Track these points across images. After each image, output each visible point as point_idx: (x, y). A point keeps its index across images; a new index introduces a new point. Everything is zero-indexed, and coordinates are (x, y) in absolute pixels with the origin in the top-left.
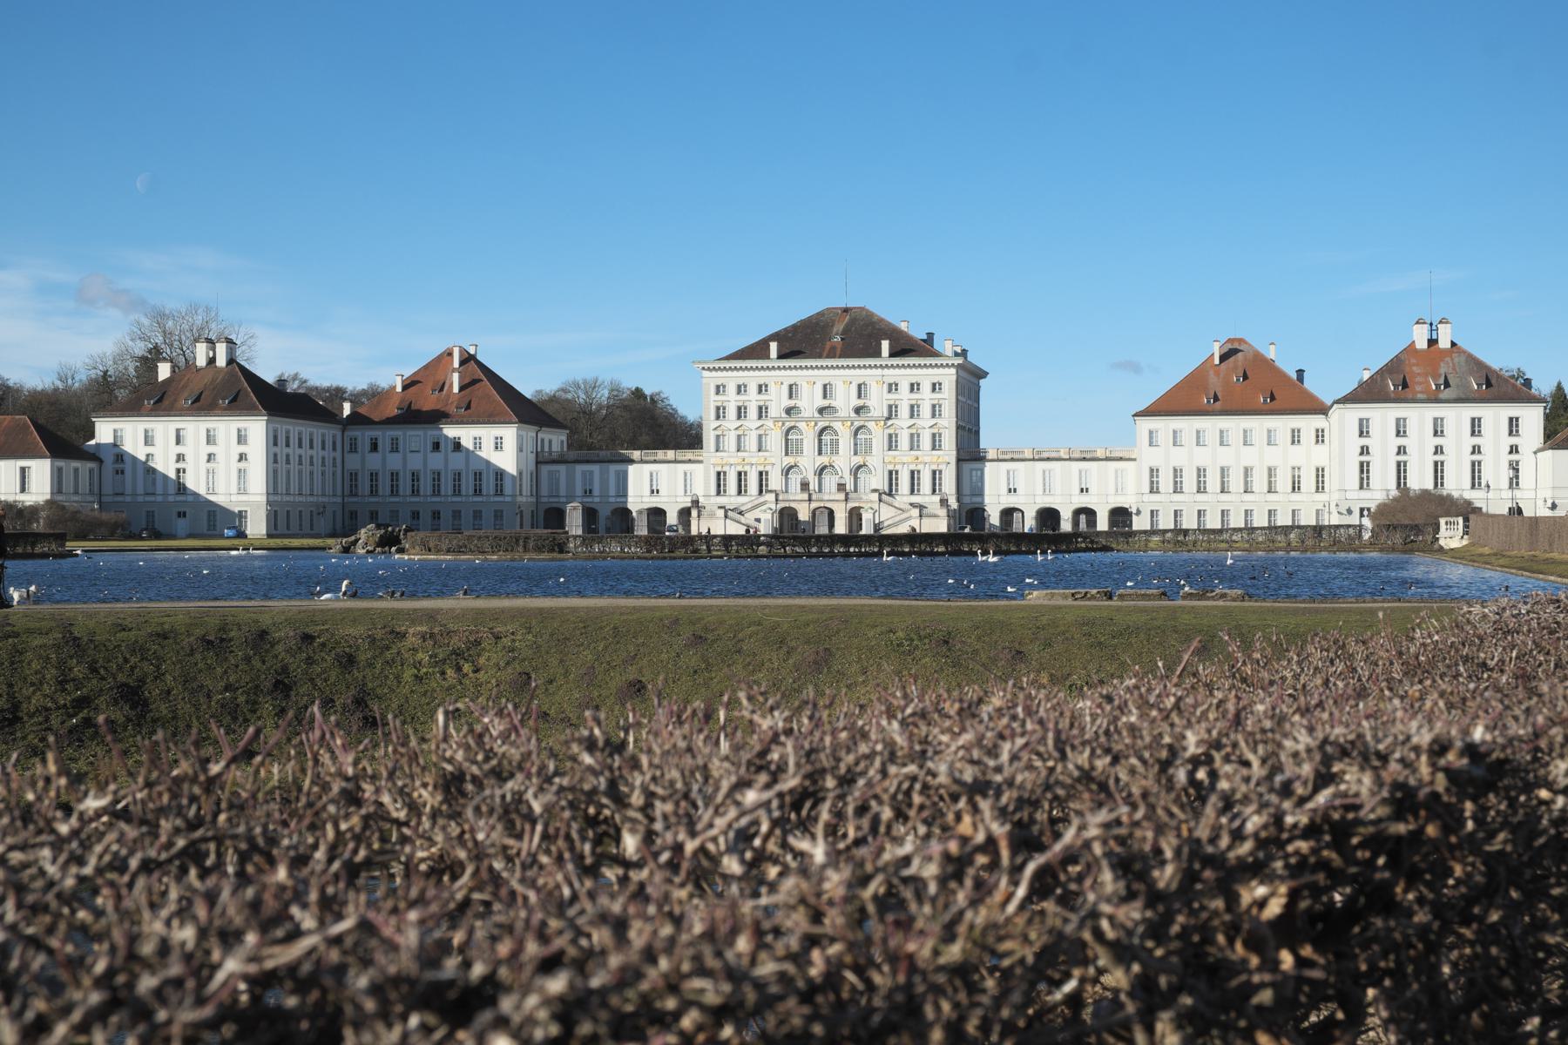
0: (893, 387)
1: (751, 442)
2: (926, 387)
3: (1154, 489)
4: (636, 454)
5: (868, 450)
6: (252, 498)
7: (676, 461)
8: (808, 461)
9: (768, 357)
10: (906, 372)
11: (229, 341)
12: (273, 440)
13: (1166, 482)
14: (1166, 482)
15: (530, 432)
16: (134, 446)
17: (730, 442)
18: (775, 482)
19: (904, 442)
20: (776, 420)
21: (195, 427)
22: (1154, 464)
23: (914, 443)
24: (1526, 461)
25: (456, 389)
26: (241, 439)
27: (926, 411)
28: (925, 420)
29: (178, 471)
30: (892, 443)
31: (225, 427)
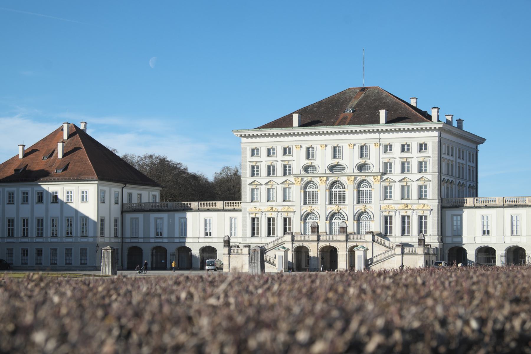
1: (278, 194)
4: (195, 205)
5: (369, 200)
7: (223, 210)
9: (291, 125)
15: (113, 189)
18: (296, 226)
23: (404, 194)
25: (60, 156)
27: (414, 167)
28: (414, 175)
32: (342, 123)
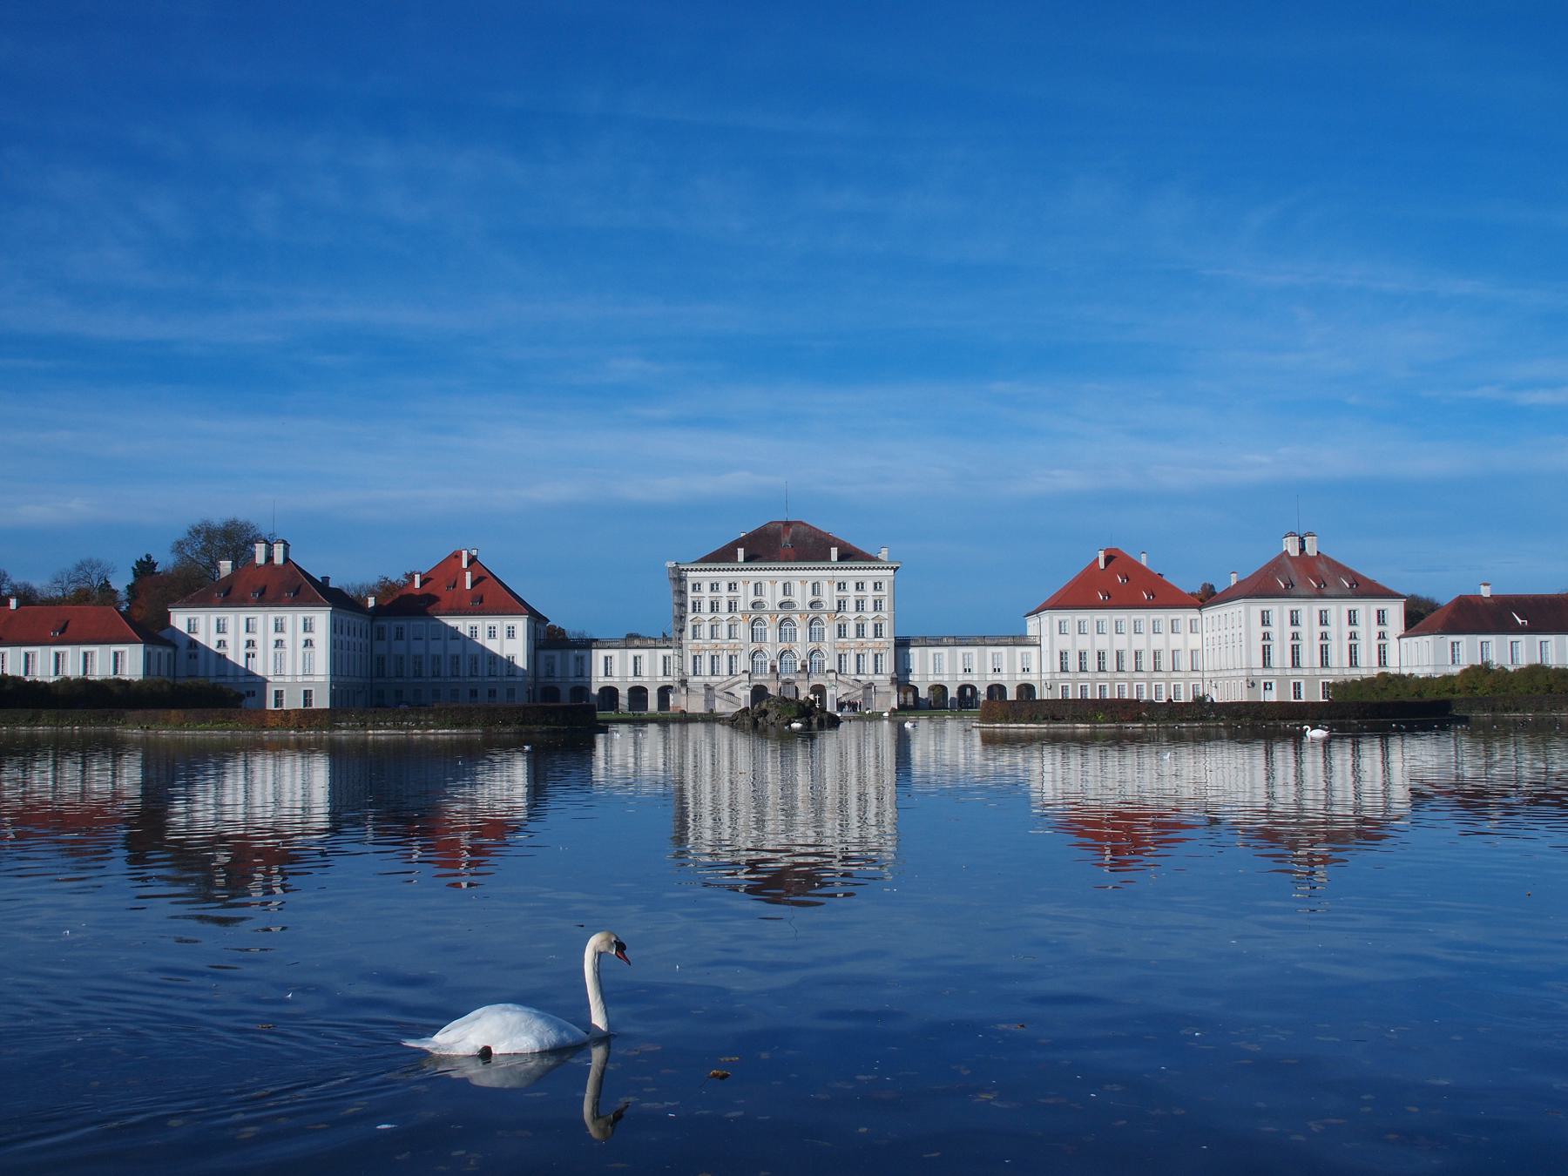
0: (841, 586)
1: (723, 631)
2: (869, 586)
3: (1063, 669)
6: (317, 679)
8: (771, 649)
10: (851, 575)
11: (284, 542)
12: (335, 628)
13: (1073, 663)
14: (1073, 663)
16: (206, 636)
17: (705, 631)
19: (851, 630)
20: (743, 613)
21: (264, 618)
22: (1064, 648)
23: (860, 632)
24: (1392, 646)
25: (468, 586)
26: (308, 627)
27: (869, 605)
28: (869, 614)
29: (248, 656)
30: (841, 632)
31: (293, 617)
32: (787, 560)
